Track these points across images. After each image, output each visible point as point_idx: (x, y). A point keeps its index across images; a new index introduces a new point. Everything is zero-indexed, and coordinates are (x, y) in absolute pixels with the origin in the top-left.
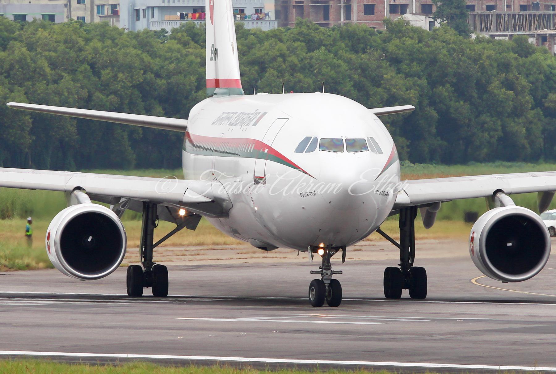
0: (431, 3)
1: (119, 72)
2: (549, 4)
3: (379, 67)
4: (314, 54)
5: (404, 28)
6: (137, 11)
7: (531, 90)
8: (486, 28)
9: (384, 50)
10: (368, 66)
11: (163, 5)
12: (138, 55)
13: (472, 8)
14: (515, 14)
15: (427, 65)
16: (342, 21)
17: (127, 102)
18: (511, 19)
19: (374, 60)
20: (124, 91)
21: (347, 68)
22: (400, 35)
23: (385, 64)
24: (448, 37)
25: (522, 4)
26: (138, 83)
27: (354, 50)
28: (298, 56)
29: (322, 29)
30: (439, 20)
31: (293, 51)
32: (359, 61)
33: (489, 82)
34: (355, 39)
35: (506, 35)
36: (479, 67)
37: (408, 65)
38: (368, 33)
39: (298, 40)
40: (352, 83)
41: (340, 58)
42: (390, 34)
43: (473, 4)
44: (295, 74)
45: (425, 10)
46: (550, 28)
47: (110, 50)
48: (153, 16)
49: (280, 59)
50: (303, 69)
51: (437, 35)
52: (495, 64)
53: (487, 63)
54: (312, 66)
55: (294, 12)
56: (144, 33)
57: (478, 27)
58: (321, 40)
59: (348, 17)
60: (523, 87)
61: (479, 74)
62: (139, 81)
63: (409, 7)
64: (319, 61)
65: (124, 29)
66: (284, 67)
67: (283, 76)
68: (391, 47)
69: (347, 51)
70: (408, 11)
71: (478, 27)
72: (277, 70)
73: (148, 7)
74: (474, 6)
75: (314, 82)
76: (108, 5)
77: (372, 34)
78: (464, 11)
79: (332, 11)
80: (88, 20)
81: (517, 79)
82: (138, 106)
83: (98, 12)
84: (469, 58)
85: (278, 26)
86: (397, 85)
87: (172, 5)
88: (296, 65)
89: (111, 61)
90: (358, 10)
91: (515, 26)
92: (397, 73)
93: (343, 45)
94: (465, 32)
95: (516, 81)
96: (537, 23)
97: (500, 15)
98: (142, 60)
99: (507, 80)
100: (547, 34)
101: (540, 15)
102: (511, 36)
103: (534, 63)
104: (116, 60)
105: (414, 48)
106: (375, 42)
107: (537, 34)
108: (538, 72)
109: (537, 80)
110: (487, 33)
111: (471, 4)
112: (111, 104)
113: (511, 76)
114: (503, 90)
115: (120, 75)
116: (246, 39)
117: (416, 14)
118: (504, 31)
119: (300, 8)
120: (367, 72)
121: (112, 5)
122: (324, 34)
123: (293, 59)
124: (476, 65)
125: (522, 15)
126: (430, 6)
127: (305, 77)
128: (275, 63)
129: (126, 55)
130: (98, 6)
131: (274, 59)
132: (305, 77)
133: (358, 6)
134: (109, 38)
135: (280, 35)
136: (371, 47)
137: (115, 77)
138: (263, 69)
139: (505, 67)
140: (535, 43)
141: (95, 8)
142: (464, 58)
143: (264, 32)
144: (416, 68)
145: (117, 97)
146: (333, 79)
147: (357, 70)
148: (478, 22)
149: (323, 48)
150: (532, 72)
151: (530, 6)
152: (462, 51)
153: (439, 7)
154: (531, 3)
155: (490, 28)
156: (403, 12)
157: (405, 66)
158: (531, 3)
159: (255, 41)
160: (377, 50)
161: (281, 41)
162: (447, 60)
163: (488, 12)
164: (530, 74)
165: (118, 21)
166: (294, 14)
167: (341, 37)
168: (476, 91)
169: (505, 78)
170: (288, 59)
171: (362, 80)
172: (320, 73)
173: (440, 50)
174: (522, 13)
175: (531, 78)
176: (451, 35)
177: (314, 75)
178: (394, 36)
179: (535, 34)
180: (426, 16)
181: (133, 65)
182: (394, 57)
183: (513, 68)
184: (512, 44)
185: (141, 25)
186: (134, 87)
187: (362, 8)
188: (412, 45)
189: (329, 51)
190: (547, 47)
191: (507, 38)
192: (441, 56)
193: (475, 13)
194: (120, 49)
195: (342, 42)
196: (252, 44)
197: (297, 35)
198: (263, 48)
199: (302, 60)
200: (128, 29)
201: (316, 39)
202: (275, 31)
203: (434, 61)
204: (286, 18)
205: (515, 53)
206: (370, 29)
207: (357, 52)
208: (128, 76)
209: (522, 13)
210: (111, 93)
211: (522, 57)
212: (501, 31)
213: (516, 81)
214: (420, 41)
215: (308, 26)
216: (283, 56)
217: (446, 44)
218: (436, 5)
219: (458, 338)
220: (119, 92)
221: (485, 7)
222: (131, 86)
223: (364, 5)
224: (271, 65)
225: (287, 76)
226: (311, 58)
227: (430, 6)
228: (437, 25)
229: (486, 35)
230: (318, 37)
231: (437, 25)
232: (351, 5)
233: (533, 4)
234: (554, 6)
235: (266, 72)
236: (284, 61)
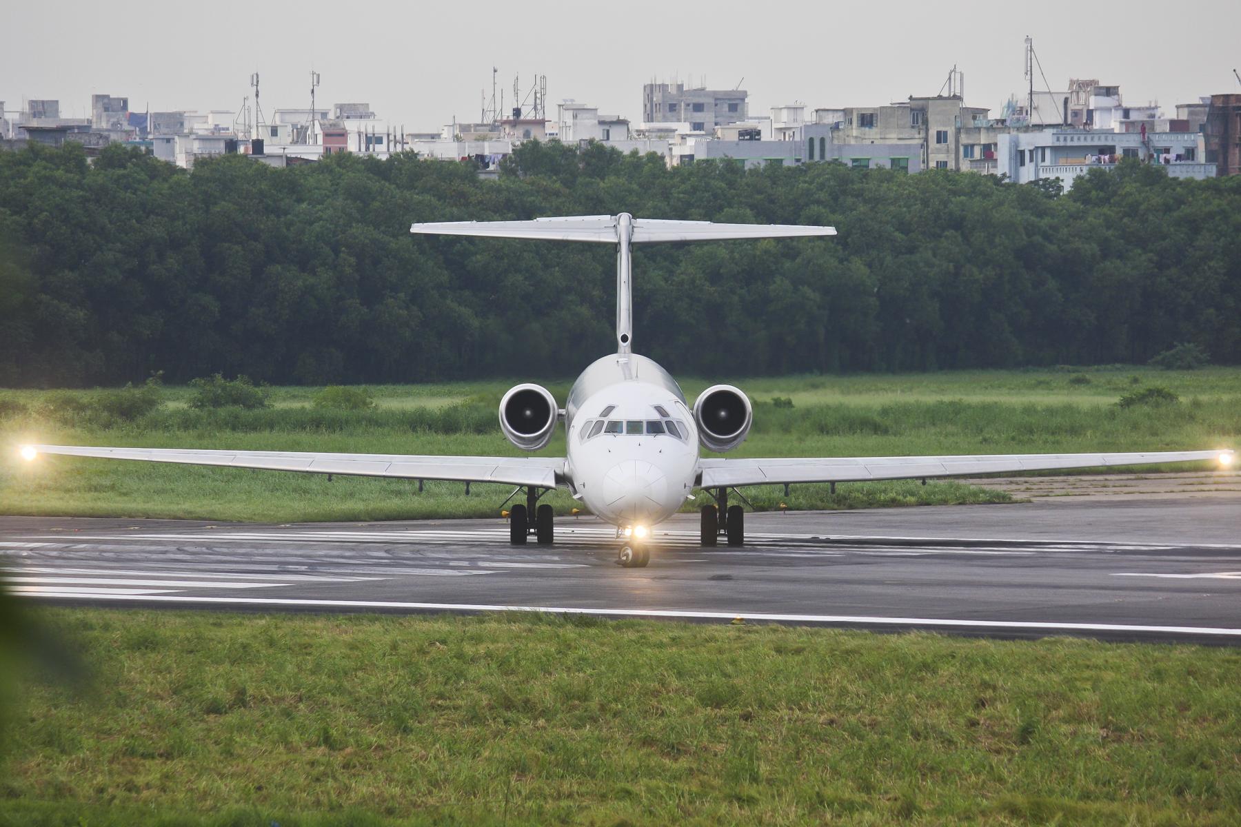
6: (1022, 153)
11: (1057, 144)
48: (1043, 160)
80: (951, 165)
83: (966, 155)
87: (1069, 143)
141: (962, 149)
165: (995, 167)
185: (1027, 175)
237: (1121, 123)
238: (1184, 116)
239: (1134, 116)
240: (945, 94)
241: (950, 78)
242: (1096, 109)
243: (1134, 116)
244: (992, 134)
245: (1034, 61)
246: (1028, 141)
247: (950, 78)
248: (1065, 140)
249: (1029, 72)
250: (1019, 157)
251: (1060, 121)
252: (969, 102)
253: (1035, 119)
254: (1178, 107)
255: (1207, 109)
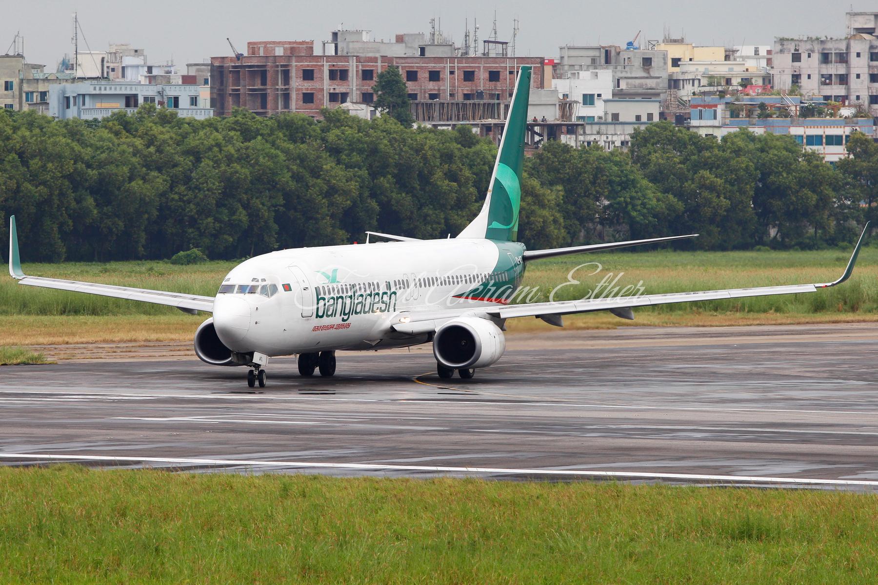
0: (372, 92)
1: (49, 161)
2: (493, 93)
3: (318, 157)
4: (249, 144)
5: (343, 117)
6: (68, 98)
7: (475, 182)
8: (429, 118)
9: (323, 139)
10: (307, 157)
11: (94, 92)
12: (68, 144)
13: (414, 96)
14: (459, 103)
15: (367, 156)
16: (280, 110)
17: (57, 192)
18: (455, 108)
19: (314, 151)
20: (53, 182)
21: (285, 158)
22: (338, 124)
23: (325, 155)
24: (388, 126)
25: (466, 92)
26: (68, 173)
27: (293, 139)
28: (233, 145)
29: (258, 118)
30: (380, 109)
31: (229, 140)
32: (298, 151)
33: (431, 173)
34: (293, 128)
35: (449, 125)
36: (422, 157)
37: (348, 155)
38: (306, 122)
39: (235, 130)
40: (290, 174)
41: (278, 148)
42: (328, 124)
43: (415, 92)
44: (232, 165)
45: (366, 98)
46: (494, 118)
47: (39, 139)
48: (84, 104)
49: (216, 149)
50: (239, 159)
51: (377, 125)
52: (438, 155)
53: (430, 153)
54: (248, 156)
55: (230, 101)
56: (73, 121)
57: (421, 116)
58: (258, 130)
59: (287, 105)
60: (468, 179)
61: (421, 164)
62: (69, 171)
63: (350, 95)
64: (256, 151)
65: (54, 118)
66: (220, 157)
67: (219, 167)
68: (332, 136)
69: (285, 141)
70: (348, 99)
71: (421, 116)
72: (213, 160)
73: (79, 95)
74: (416, 94)
75: (251, 173)
76: (38, 92)
77: (310, 124)
78: (406, 99)
79: (270, 99)
80: (16, 107)
81: (461, 170)
82: (68, 197)
83: (27, 100)
84: (412, 149)
85: (214, 115)
86: (336, 176)
87: (103, 92)
88: (232, 156)
89: (40, 150)
90: (297, 98)
91: (458, 115)
92: (337, 164)
93: (281, 135)
94: (407, 121)
95: (459, 173)
96: (481, 112)
97: (443, 104)
98: (73, 149)
99: (450, 171)
100: (491, 124)
101: (484, 104)
102: (454, 125)
103: (477, 153)
104: (46, 149)
105: (354, 138)
106: (314, 131)
107: (481, 124)
108: (482, 163)
109: (481, 171)
110: (430, 122)
111: (413, 92)
112: (40, 195)
113: (454, 167)
114: (447, 182)
115: (50, 165)
116: (180, 128)
117: (356, 103)
118: (448, 120)
119: (236, 96)
120: (306, 163)
121: (41, 92)
122: (261, 123)
123: (231, 149)
124: (418, 155)
125: (466, 104)
126: (371, 95)
127: (242, 167)
128: (210, 153)
129: (55, 144)
130: (27, 94)
131: (210, 149)
132: (242, 167)
133: (296, 94)
134: (37, 127)
135: (216, 124)
136: (310, 137)
137: (44, 167)
138: (198, 160)
139: (448, 157)
140: (479, 133)
141: (24, 95)
142: (405, 149)
143: (199, 121)
144: (356, 158)
145: (46, 187)
146: (270, 169)
147: (296, 160)
148: (420, 111)
149: (259, 138)
150: (475, 163)
151: (473, 94)
152: (404, 141)
153: (380, 96)
154: (475, 92)
155: (433, 117)
156: (343, 101)
157: (344, 157)
158: (475, 92)
159: (190, 130)
160: (316, 141)
161: (217, 131)
162: (388, 151)
163: (430, 101)
164: (474, 165)
165: (48, 109)
166: (231, 103)
167: (278, 126)
168: (418, 182)
169: (448, 169)
170: (224, 149)
171: (301, 170)
172: (257, 163)
173: (381, 139)
174: (465, 102)
175: (475, 169)
176: (394, 125)
177: (251, 166)
178: (332, 125)
179: (478, 124)
180: (367, 105)
181: (63, 154)
182: (334, 146)
183: (456, 158)
184: (456, 134)
185: (72, 113)
186: (63, 177)
187: (301, 96)
188: (352, 134)
189: (267, 141)
190: (491, 136)
191: (450, 128)
192: (382, 146)
193: (416, 101)
194: (49, 137)
195: (280, 132)
196: (187, 133)
197: (233, 123)
198: (197, 138)
199: (239, 150)
200: (58, 117)
201: (252, 128)
202: (210, 120)
203: (374, 151)
204: (222, 107)
205: (458, 144)
206: (308, 118)
207: (295, 142)
208: (58, 166)
209: (465, 102)
210: (40, 184)
211: (465, 147)
212: (444, 121)
213: (459, 173)
214: (359, 131)
215: (245, 115)
216: (218, 145)
217: (387, 134)
218: (377, 94)
219: (398, 439)
220: (48, 183)
221: (427, 95)
222: (62, 177)
223: (304, 94)
224: (207, 155)
225: (223, 167)
226: (247, 148)
227: (371, 95)
228: (378, 114)
229: (428, 125)
230: (255, 126)
231: (378, 114)
232: (289, 93)
233: (477, 92)
234: (498, 94)
235: (201, 162)
236: (221, 150)
237: (146, 77)
238: (192, 72)
239: (155, 72)
240: (11, 53)
241: (15, 42)
242: (127, 67)
243: (155, 72)
244: (46, 84)
245: (78, 29)
246: (72, 90)
247: (15, 42)
248: (100, 89)
249: (75, 38)
250: (66, 102)
251: (99, 74)
252: (30, 60)
253: (79, 73)
254: (188, 65)
255: (209, 67)
